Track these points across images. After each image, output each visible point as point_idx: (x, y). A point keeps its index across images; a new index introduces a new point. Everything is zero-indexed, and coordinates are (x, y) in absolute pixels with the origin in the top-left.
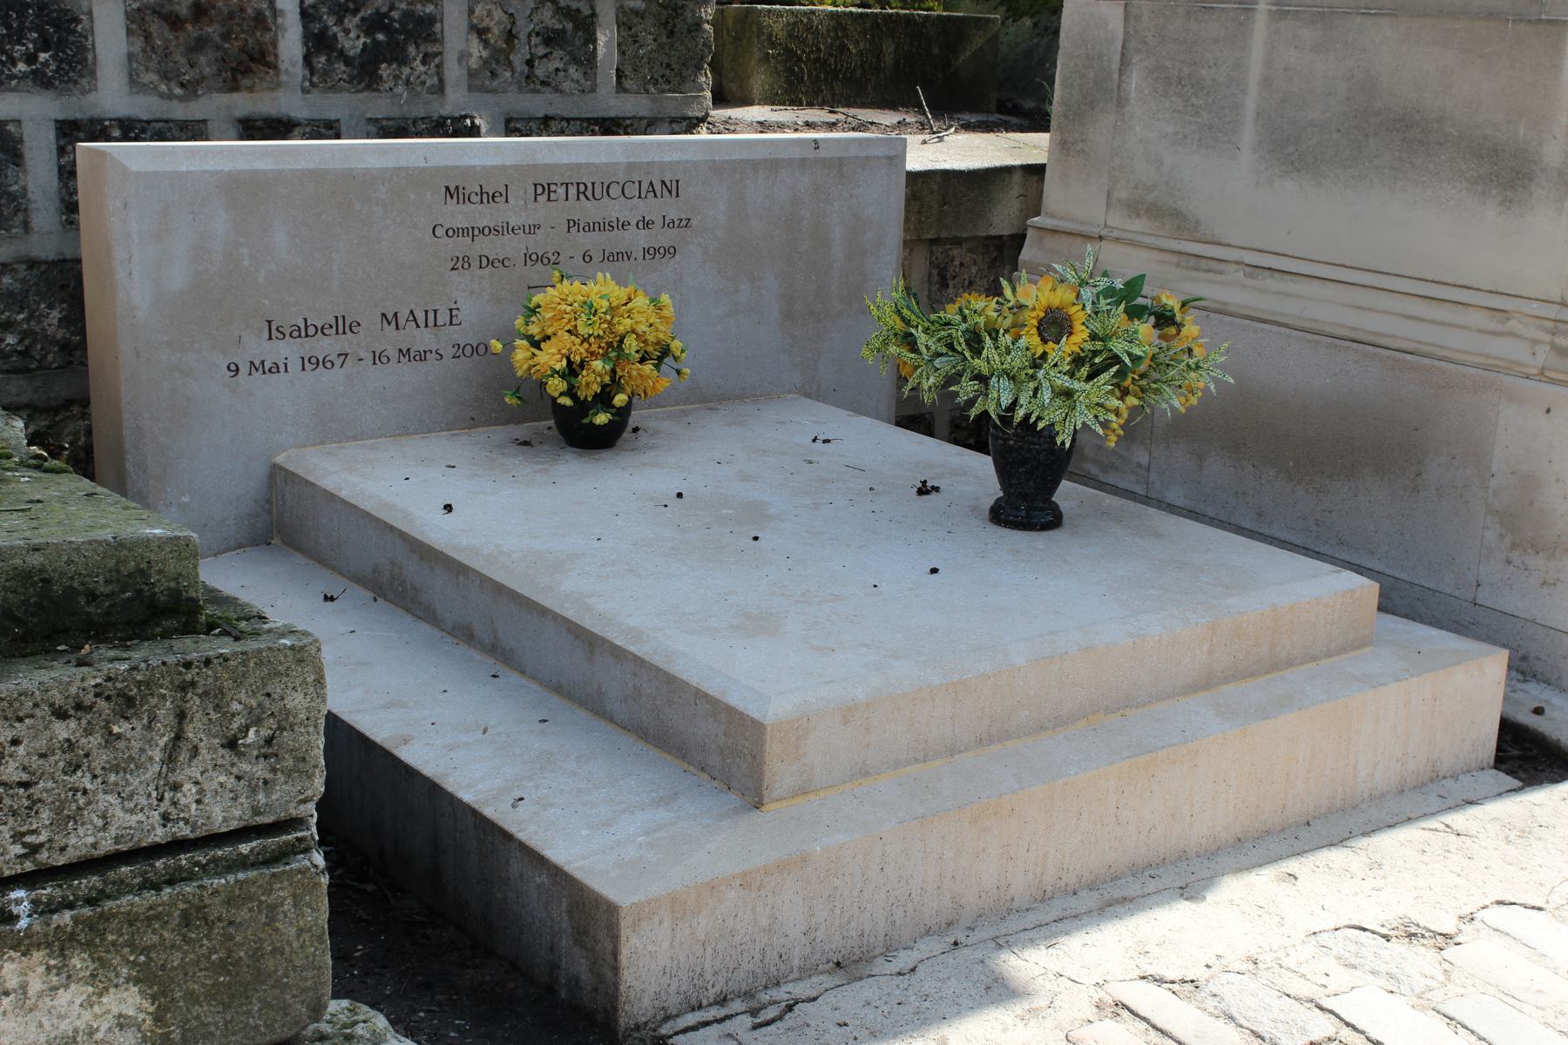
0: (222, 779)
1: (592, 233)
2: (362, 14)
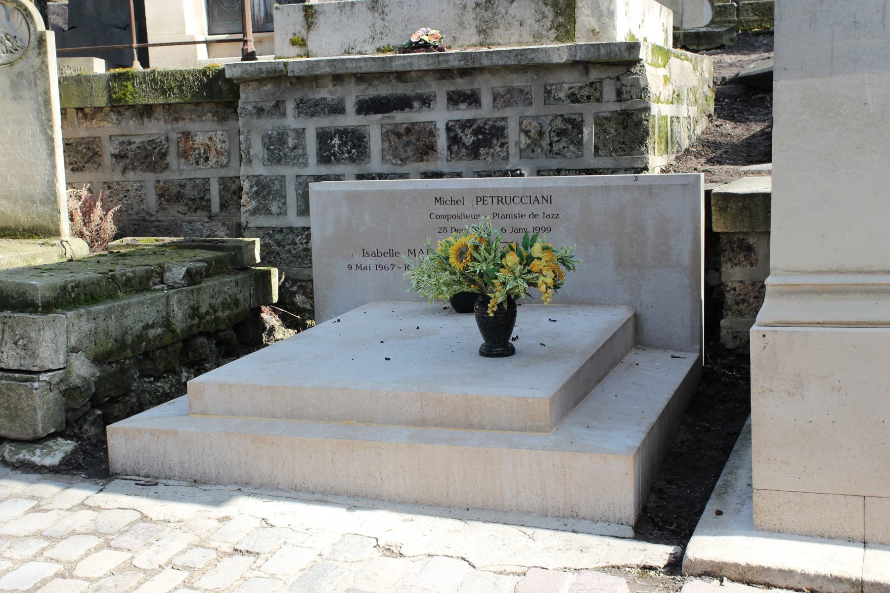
0: (13, 353)
2: (473, 128)
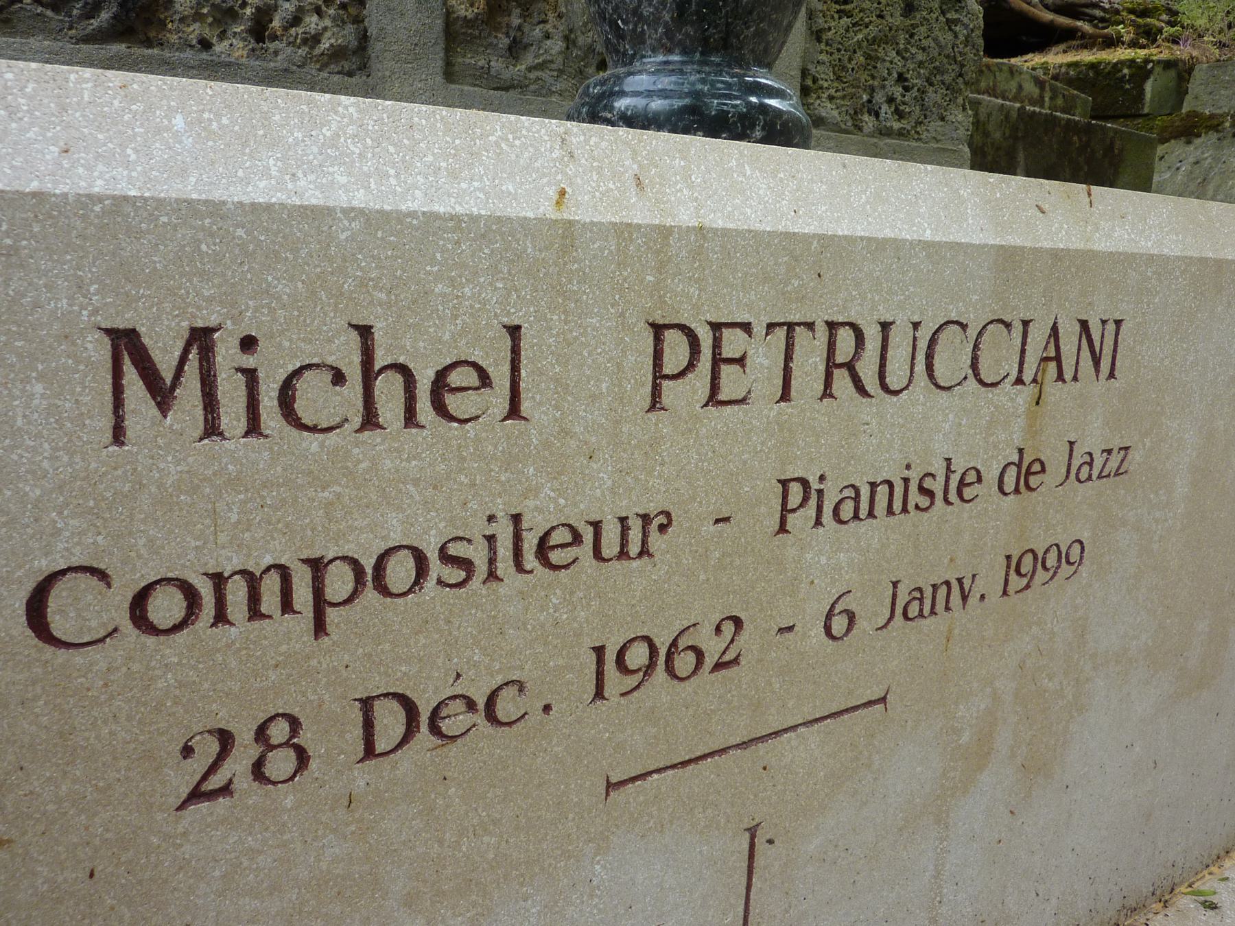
1: (864, 527)
